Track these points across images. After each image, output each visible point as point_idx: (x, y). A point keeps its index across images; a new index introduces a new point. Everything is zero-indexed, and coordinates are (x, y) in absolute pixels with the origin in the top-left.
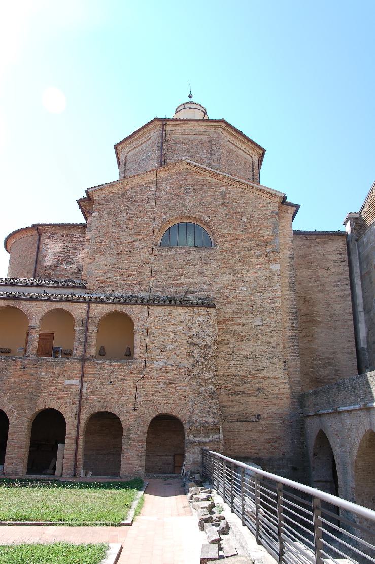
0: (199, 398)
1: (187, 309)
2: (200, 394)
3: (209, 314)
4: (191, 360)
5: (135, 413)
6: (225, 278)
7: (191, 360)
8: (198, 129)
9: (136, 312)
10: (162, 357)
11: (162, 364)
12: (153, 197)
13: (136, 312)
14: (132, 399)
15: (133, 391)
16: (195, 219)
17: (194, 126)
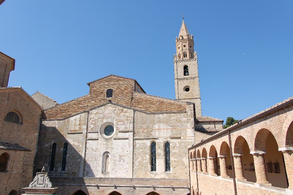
0: (22, 183)
1: (24, 152)
2: (23, 182)
3: (29, 154)
4: (22, 170)
5: (6, 191)
6: (23, 136)
7: (22, 170)
8: (3, 58)
9: (11, 153)
10: (16, 170)
11: (15, 172)
12: (6, 99)
13: (11, 153)
14: (5, 186)
15: (6, 183)
16: (18, 112)
17: (2, 56)
